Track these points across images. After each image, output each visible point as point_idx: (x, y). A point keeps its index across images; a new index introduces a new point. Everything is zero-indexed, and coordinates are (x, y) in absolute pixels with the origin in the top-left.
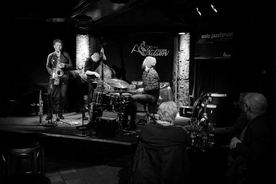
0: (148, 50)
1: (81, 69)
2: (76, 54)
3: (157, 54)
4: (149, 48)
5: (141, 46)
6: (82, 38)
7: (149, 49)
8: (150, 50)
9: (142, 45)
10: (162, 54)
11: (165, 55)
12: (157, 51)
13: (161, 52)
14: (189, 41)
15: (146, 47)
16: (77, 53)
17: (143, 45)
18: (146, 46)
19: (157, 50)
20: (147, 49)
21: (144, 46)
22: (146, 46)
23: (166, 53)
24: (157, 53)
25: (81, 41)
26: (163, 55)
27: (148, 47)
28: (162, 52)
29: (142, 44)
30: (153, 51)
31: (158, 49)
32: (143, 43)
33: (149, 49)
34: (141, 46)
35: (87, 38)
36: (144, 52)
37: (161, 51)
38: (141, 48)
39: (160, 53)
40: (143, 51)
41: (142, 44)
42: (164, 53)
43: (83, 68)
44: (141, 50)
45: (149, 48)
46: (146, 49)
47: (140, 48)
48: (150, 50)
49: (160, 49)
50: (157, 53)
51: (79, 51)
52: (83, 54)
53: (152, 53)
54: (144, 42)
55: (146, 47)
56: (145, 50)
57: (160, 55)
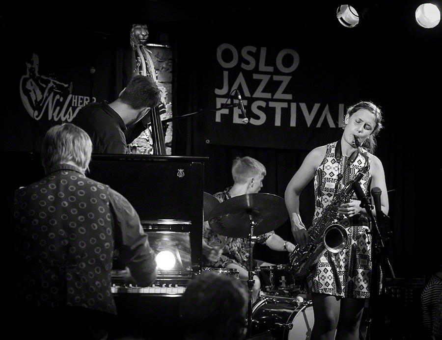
0: (46, 94)
5: (28, 73)
8: (52, 94)
14: (170, 75)
17: (32, 70)
18: (42, 77)
19: (70, 96)
20: (46, 88)
21: (37, 75)
22: (42, 77)
24: (70, 109)
29: (29, 66)
30: (61, 100)
31: (73, 94)
32: (32, 63)
34: (28, 73)
36: (36, 101)
37: (80, 101)
38: (28, 86)
40: (34, 98)
44: (27, 92)
46: (43, 90)
47: (26, 80)
48: (52, 94)
49: (78, 95)
50: (70, 109)
53: (58, 108)
54: (35, 58)
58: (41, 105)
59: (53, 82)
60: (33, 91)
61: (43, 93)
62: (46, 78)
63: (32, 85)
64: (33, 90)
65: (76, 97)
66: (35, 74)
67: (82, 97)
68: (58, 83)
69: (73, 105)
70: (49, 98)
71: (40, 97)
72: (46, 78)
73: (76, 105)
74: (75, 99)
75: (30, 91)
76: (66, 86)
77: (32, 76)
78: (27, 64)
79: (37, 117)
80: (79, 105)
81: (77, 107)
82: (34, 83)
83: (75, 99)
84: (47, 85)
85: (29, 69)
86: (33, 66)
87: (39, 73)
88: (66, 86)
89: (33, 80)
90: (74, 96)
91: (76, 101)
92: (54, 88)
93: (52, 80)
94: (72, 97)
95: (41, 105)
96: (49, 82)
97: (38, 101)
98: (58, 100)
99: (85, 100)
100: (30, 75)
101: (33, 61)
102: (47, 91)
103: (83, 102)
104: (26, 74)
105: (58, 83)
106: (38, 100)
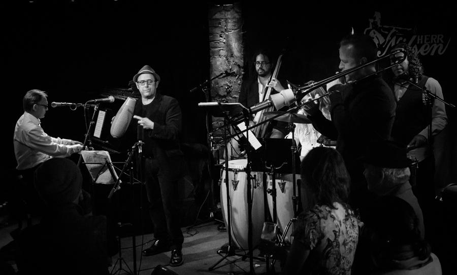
1: (225, 96)
2: (210, 56)
3: (417, 49)
4: (393, 30)
6: (223, 12)
7: (392, 37)
8: (395, 38)
9: (375, 24)
10: (428, 49)
11: (440, 54)
12: (417, 38)
13: (426, 43)
15: (385, 29)
16: (211, 54)
17: (375, 24)
19: (414, 38)
20: (388, 34)
23: (441, 46)
24: (415, 47)
25: (223, 22)
26: (432, 54)
27: (389, 30)
28: (431, 45)
29: (371, 21)
30: (405, 40)
32: (375, 18)
33: (392, 37)
35: (238, 11)
36: (379, 44)
39: (424, 46)
41: (371, 21)
42: (436, 47)
43: (230, 92)
45: (393, 30)
46: (385, 36)
47: (369, 32)
48: (395, 38)
50: (415, 47)
51: (216, 49)
52: (229, 54)
54: (378, 15)
55: (385, 29)
56: (382, 41)
57: (424, 54)
58: (384, 46)
59: (395, 29)
60: (375, 37)
61: (385, 38)
62: (388, 27)
63: (375, 34)
64: (376, 37)
65: (422, 36)
66: (378, 26)
67: (429, 36)
68: (400, 28)
69: (418, 43)
70: (392, 40)
71: (382, 41)
72: (388, 27)
73: (422, 42)
74: (420, 38)
75: (374, 38)
76: (410, 29)
77: (375, 27)
78: (370, 20)
79: (380, 55)
80: (425, 42)
81: (423, 44)
82: (376, 32)
83: (420, 38)
84: (389, 32)
85: (372, 23)
86: (376, 20)
87: (381, 24)
88: (410, 29)
89: (376, 30)
90: (419, 36)
91: (422, 39)
92: (397, 33)
93: (394, 28)
94: (417, 38)
95: (384, 46)
96: (392, 28)
97: (381, 43)
98: (401, 40)
99: (432, 37)
100: (373, 27)
101: (375, 17)
102: (389, 36)
103: (430, 40)
104: (369, 27)
105: (400, 28)
106: (381, 43)
